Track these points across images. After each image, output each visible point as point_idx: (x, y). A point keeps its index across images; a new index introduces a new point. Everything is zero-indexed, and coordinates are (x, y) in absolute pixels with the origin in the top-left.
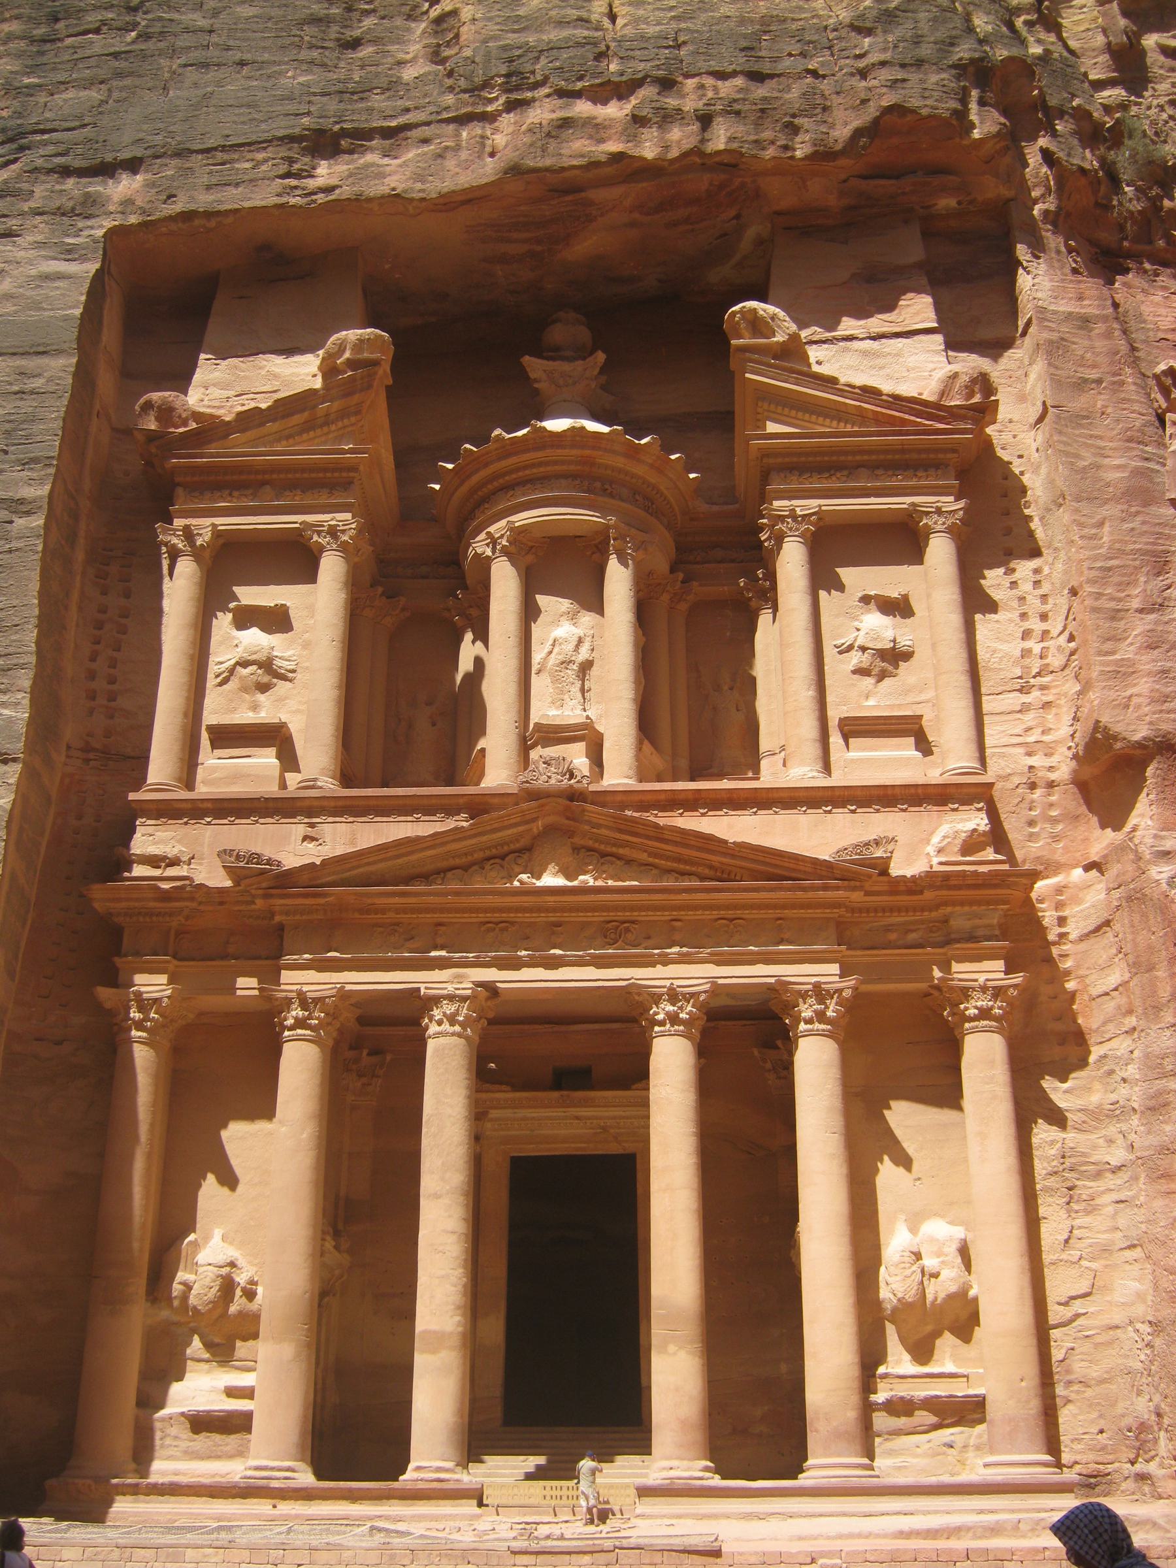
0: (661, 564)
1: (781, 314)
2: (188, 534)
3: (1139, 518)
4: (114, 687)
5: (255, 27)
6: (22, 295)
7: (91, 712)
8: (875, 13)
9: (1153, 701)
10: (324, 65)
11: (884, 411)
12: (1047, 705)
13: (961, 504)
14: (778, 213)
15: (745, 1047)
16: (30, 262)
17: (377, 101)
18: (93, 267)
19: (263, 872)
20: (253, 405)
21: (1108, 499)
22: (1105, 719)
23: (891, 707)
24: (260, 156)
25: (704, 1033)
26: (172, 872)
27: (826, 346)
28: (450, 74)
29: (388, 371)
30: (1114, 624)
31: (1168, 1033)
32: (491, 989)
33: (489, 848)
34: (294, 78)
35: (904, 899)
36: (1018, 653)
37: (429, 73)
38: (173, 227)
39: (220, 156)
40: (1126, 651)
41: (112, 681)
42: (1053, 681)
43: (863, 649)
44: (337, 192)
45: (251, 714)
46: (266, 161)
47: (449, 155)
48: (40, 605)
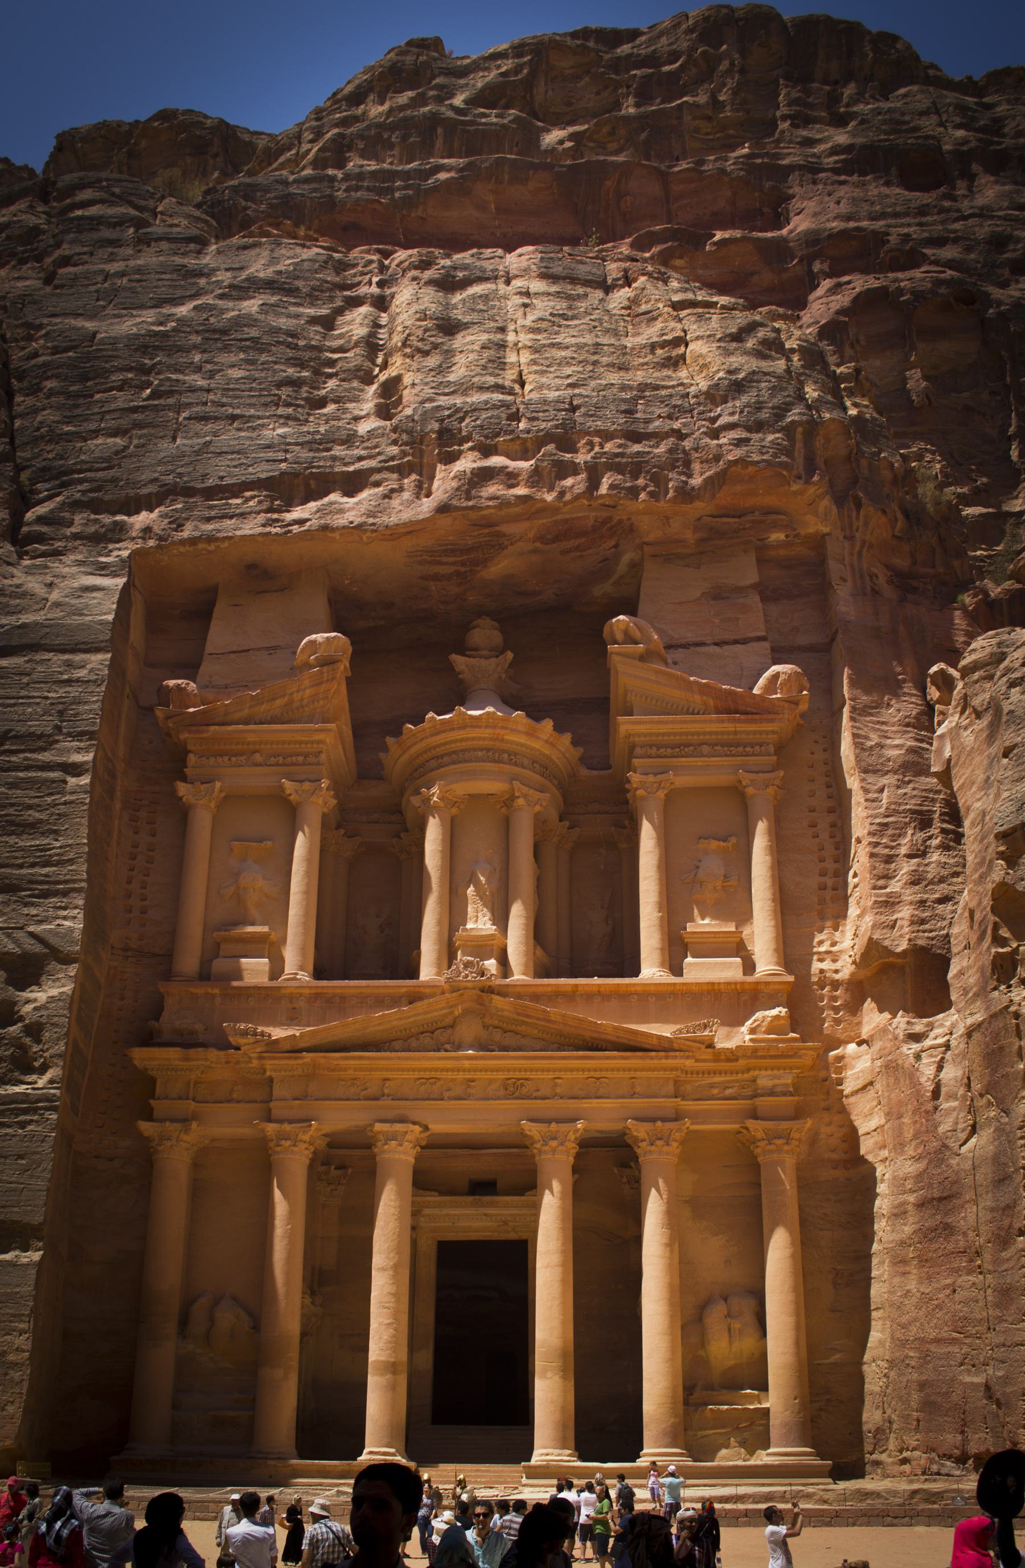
0: (553, 815)
3: (911, 785)
5: (243, 387)
6: (68, 604)
8: (726, 382)
9: (912, 923)
10: (297, 419)
15: (609, 1180)
17: (338, 451)
18: (121, 581)
22: (875, 937)
24: (248, 494)
28: (395, 430)
31: (909, 1162)
34: (274, 429)
37: (379, 428)
38: (182, 549)
40: (895, 886)
47: (394, 495)
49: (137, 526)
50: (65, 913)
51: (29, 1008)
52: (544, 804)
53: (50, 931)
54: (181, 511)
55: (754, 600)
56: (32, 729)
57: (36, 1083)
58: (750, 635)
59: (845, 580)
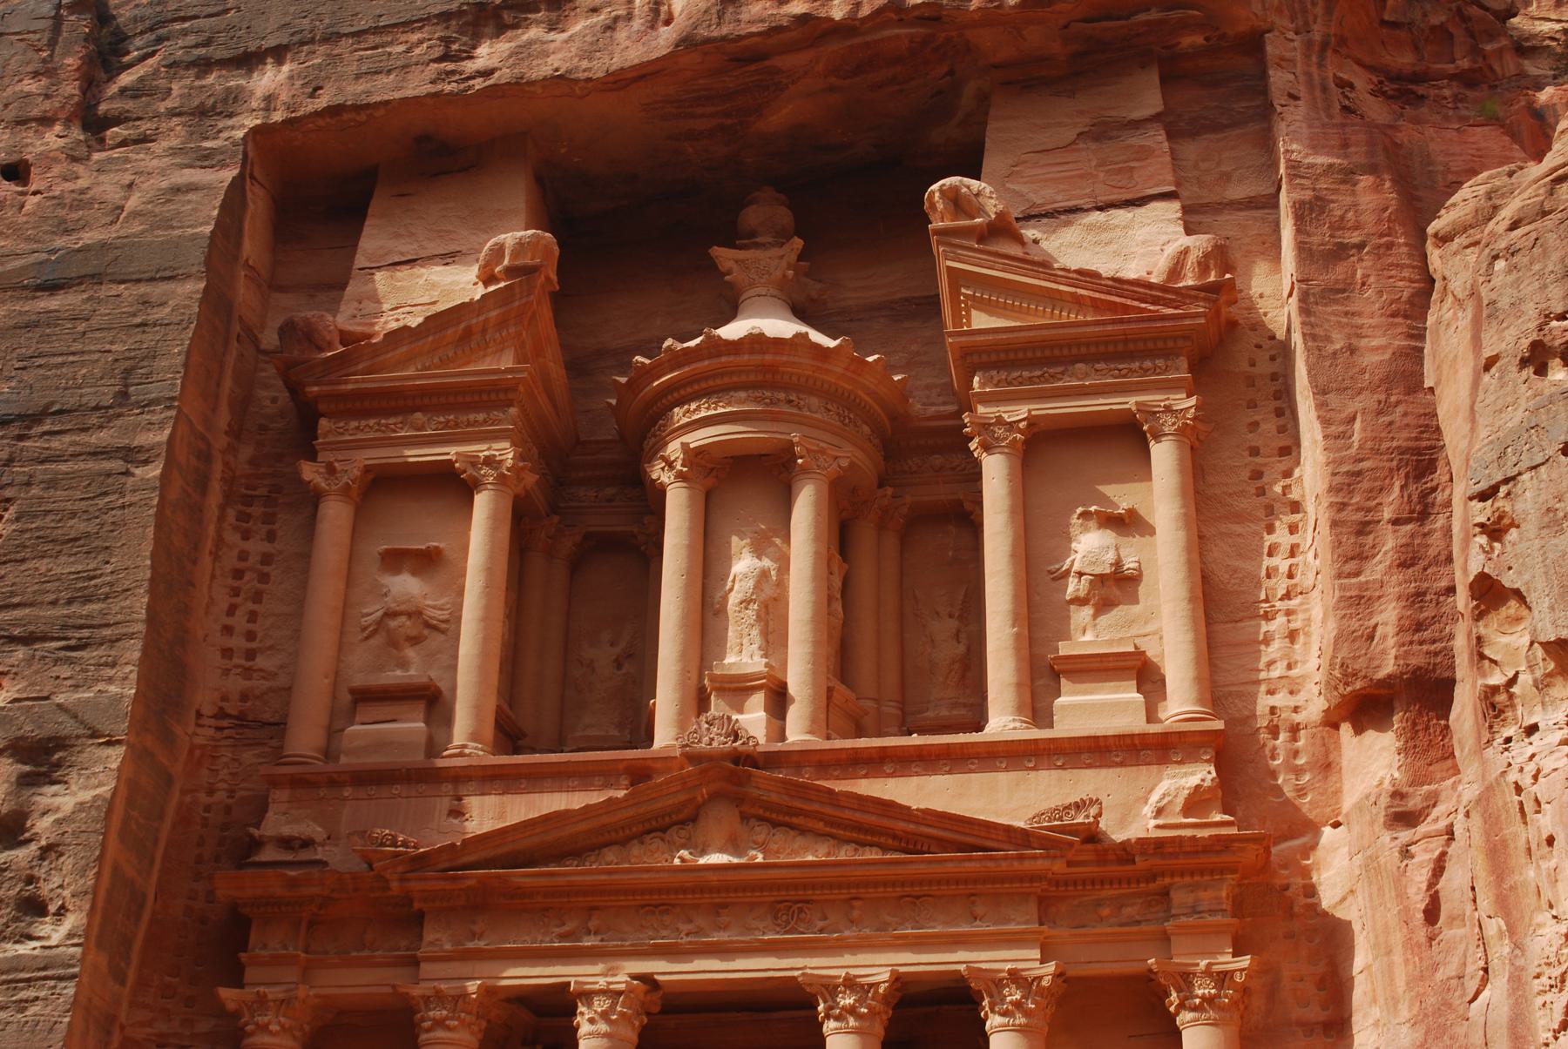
1: (989, 189)
2: (331, 470)
3: (1400, 409)
4: (254, 645)
7: (226, 672)
9: (1401, 630)
11: (1103, 296)
13: (1193, 401)
14: (996, 67)
16: (163, 172)
18: (229, 174)
19: (397, 854)
20: (401, 324)
21: (1362, 389)
23: (1111, 642)
24: (415, 37)
26: (305, 855)
27: (1045, 220)
29: (554, 277)
30: (1361, 539)
32: (646, 979)
33: (649, 820)
35: (1114, 869)
38: (321, 122)
39: (373, 39)
40: (1375, 570)
41: (251, 636)
42: (1302, 604)
43: (1080, 574)
44: (496, 75)
45: (399, 673)
46: (421, 42)
47: (620, 24)
48: (153, 567)
49: (259, 93)
50: (110, 672)
51: (47, 821)
52: (844, 463)
53: (87, 700)
54: (319, 67)
55: (1157, 138)
56: (84, 400)
57: (49, 938)
59: (1296, 98)
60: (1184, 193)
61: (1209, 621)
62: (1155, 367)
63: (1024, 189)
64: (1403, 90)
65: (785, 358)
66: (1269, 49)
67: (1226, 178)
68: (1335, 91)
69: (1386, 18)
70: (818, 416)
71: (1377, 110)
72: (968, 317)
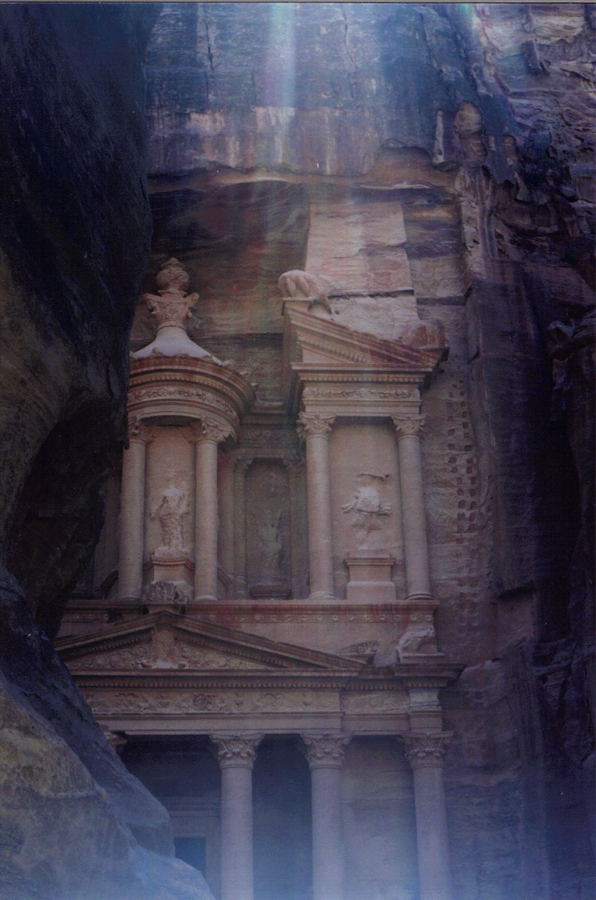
12: (473, 553)
23: (377, 552)
25: (255, 763)
27: (341, 300)
32: (121, 734)
36: (455, 516)
43: (360, 511)
55: (402, 257)
58: (400, 289)
59: (476, 242)
60: (416, 292)
61: (429, 542)
62: (403, 394)
63: (329, 279)
64: (523, 238)
65: (198, 370)
66: (464, 211)
67: (436, 284)
68: (495, 239)
69: (518, 197)
70: (213, 405)
71: (514, 254)
72: (301, 356)
